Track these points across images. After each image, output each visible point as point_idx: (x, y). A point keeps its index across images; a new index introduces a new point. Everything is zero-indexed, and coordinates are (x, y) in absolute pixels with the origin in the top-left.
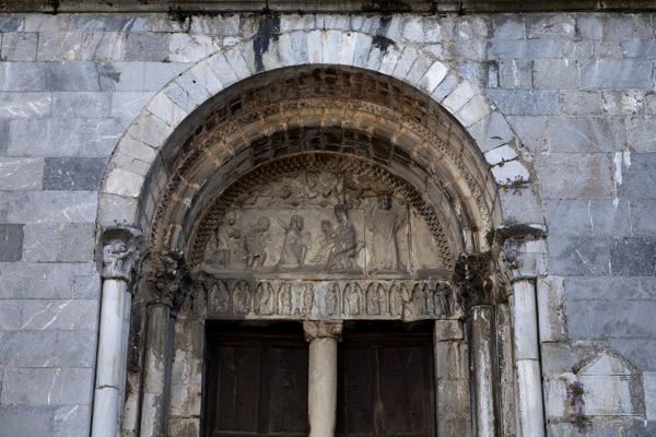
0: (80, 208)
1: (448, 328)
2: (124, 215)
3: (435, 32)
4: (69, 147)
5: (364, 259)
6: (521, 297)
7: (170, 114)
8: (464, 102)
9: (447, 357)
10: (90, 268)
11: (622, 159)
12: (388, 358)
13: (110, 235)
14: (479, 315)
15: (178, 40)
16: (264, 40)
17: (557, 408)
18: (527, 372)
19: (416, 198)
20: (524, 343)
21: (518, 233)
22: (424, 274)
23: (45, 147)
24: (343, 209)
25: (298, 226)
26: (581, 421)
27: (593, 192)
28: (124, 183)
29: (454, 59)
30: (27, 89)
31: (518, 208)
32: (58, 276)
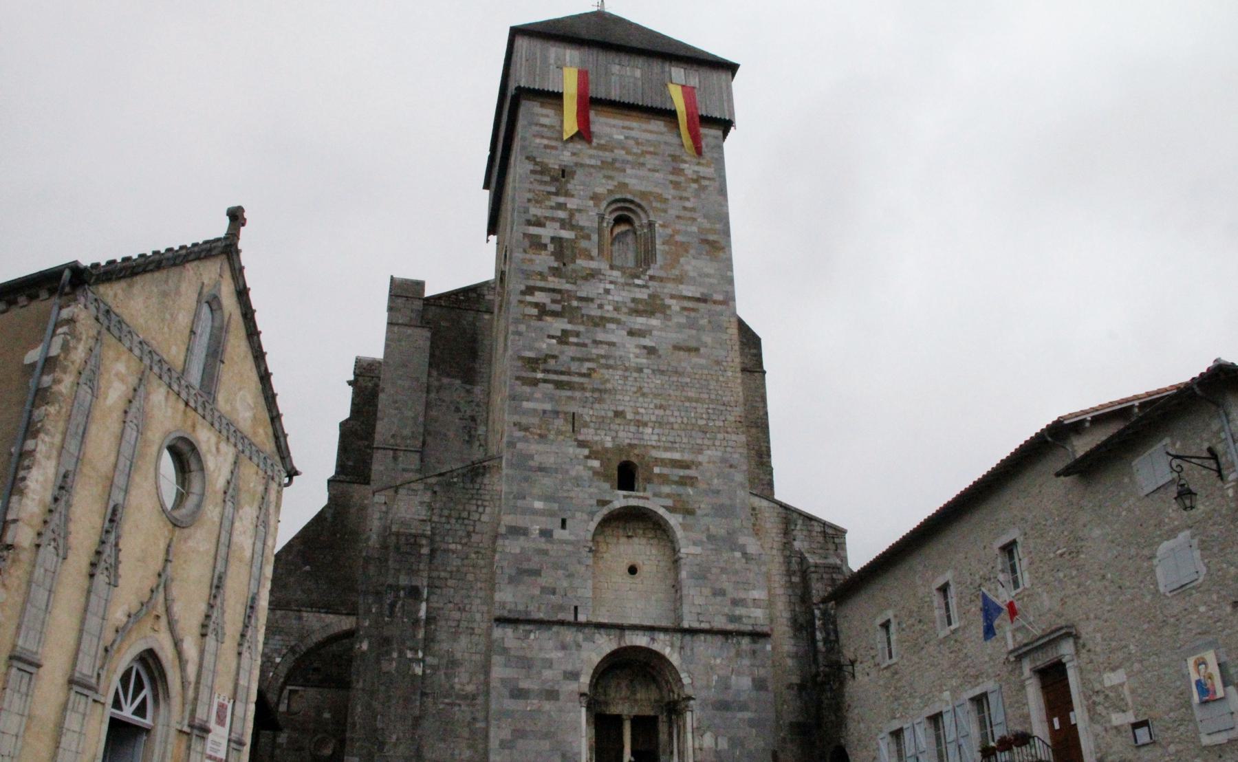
0: (573, 686)
1: (663, 718)
2: (586, 689)
3: (668, 637)
4: (569, 668)
5: (638, 696)
6: (689, 714)
7: (596, 659)
8: (675, 659)
9: (663, 728)
10: (577, 703)
11: (715, 677)
12: (644, 726)
13: (582, 695)
14: (674, 717)
15: (597, 636)
16: (621, 637)
17: (697, 746)
18: (689, 736)
19: (654, 679)
20: (689, 728)
21: (689, 698)
22: (656, 701)
23: (563, 668)
24: (632, 681)
25: (619, 684)
26: (701, 749)
27: (708, 687)
28: (585, 680)
29: (672, 646)
30: (556, 648)
31: (688, 691)
32: (570, 705)
